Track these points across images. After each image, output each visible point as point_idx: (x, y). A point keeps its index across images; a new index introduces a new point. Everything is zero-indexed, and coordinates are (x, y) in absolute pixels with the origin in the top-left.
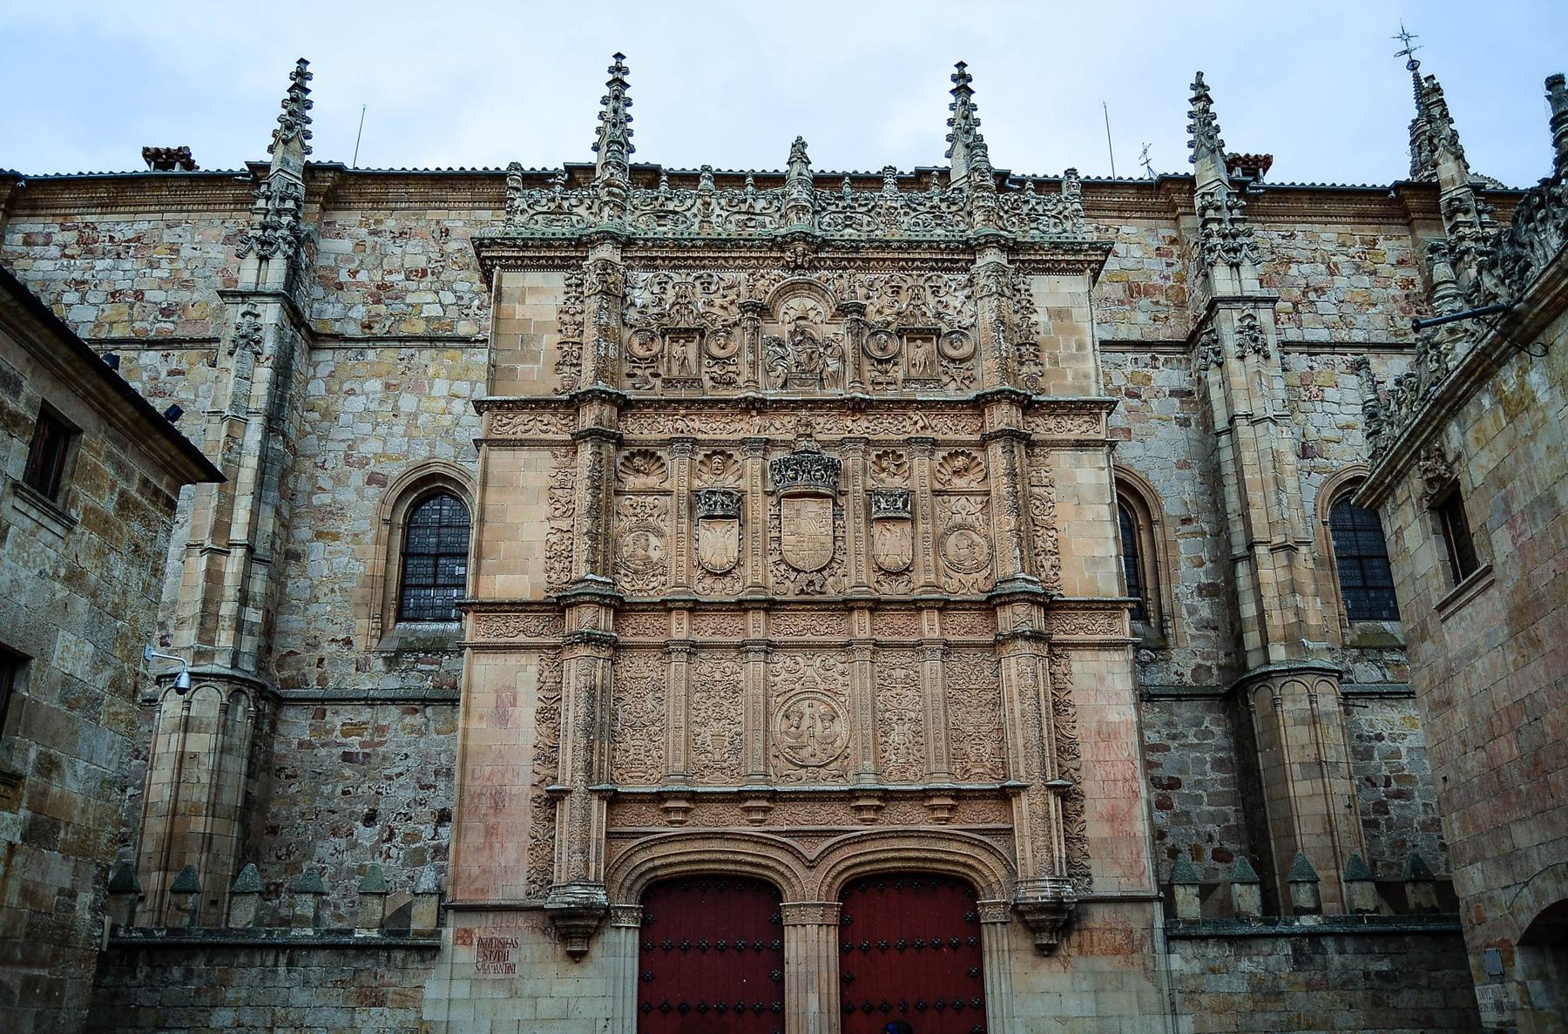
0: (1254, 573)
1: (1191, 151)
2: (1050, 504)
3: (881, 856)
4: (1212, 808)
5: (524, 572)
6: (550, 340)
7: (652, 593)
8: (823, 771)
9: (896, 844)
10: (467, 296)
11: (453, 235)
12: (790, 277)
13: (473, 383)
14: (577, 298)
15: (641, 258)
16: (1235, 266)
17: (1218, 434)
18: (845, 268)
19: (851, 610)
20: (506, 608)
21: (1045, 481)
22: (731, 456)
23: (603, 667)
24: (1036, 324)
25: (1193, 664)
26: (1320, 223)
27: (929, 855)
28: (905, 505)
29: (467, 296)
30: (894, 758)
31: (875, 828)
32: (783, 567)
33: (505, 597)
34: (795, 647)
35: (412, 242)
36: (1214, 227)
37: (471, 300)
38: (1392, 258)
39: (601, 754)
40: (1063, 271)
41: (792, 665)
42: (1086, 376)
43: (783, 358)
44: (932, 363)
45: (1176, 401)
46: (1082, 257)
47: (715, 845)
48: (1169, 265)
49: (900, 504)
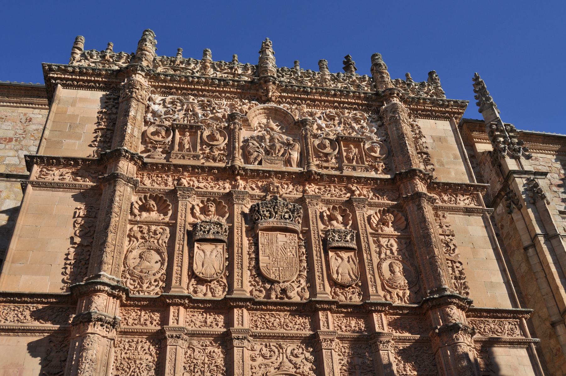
1: (478, 108)
7: (152, 293)
11: (34, 121)
12: (261, 106)
14: (114, 106)
15: (162, 87)
16: (517, 159)
17: (526, 249)
18: (299, 104)
21: (448, 233)
22: (220, 202)
26: (550, 154)
28: (352, 239)
35: (6, 123)
36: (502, 139)
41: (269, 353)
43: (258, 148)
44: (361, 158)
49: (348, 238)
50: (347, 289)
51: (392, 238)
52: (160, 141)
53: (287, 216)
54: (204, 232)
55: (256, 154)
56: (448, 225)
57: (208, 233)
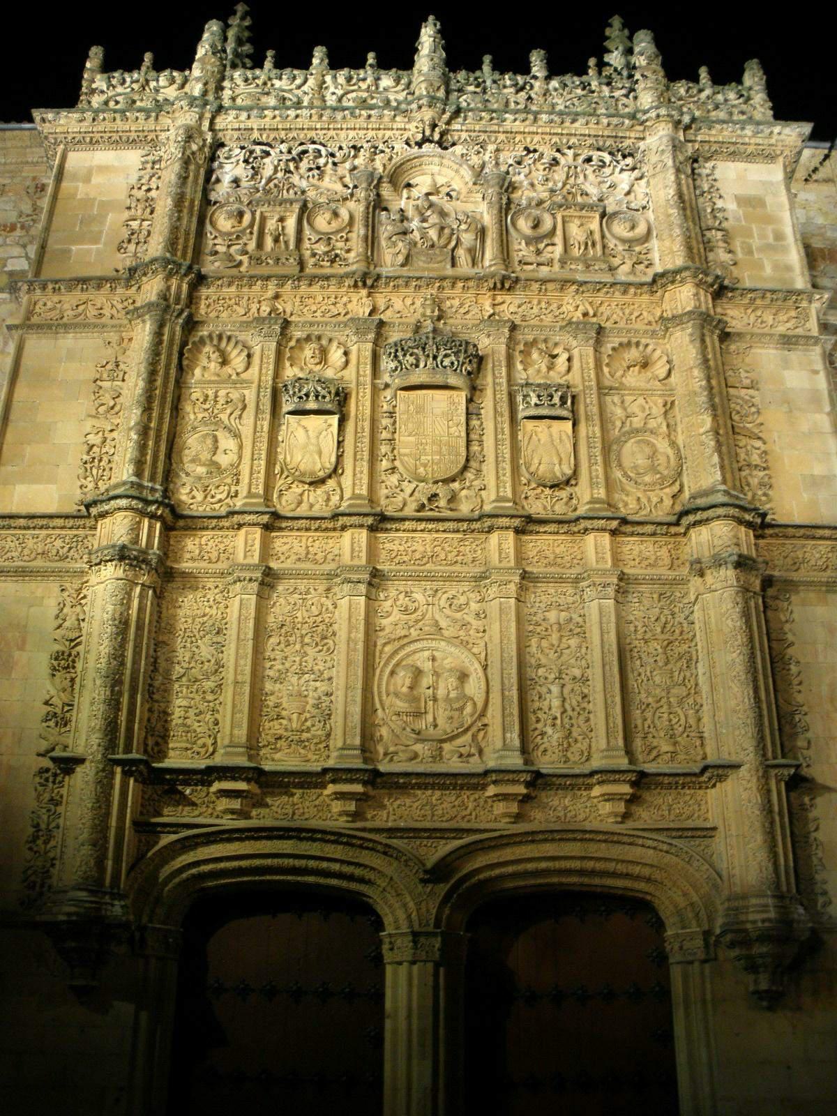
2: (753, 409)
3: (530, 866)
5: (51, 480)
6: (114, 219)
7: (217, 506)
8: (447, 746)
9: (549, 849)
19: (490, 530)
20: (22, 522)
21: (747, 382)
23: (141, 596)
27: (599, 866)
28: (563, 400)
30: (549, 730)
32: (394, 479)
33: (23, 511)
34: (410, 578)
39: (131, 712)
40: (750, 157)
42: (789, 268)
46: (773, 141)
47: (286, 846)
49: (556, 400)
50: (547, 491)
51: (641, 395)
52: (230, 234)
53: (447, 362)
54: (301, 398)
55: (400, 244)
56: (748, 369)
57: (307, 400)
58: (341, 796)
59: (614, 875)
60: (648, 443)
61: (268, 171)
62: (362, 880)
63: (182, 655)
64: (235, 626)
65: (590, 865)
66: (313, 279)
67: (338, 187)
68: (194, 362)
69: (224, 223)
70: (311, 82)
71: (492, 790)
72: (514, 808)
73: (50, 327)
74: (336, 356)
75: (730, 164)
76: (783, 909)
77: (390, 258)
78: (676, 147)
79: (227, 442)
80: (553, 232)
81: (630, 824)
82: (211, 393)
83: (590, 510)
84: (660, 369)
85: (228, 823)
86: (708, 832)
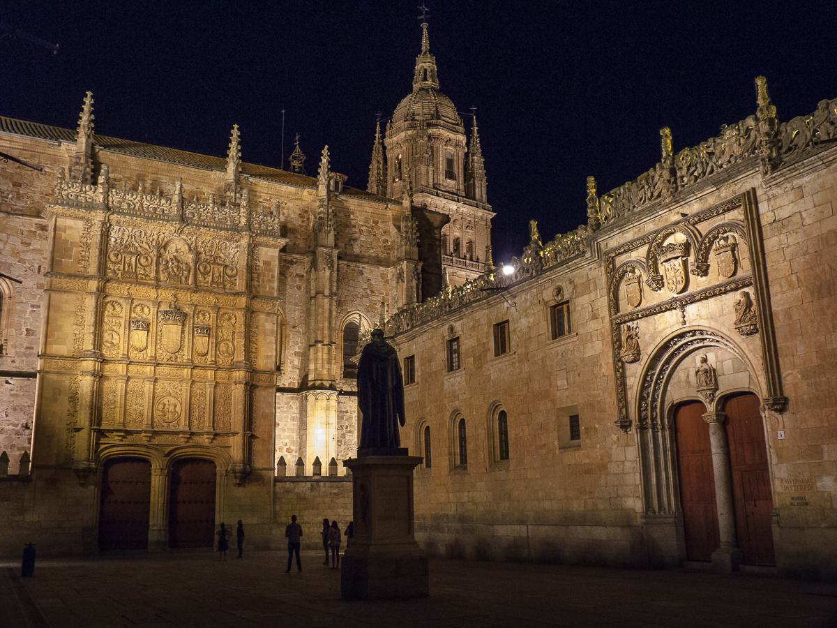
0: (316, 353)
4: (288, 434)
10: (6, 192)
13: (9, 235)
24: (259, 266)
25: (289, 382)
28: (207, 331)
29: (6, 192)
31: (187, 445)
32: (161, 351)
37: (8, 195)
38: (381, 231)
42: (273, 288)
45: (297, 279)
48: (303, 221)
52: (114, 263)
58: (146, 436)
59: (205, 455)
60: (228, 344)
61: (126, 238)
62: (149, 456)
63: (105, 399)
64: (119, 391)
65: (202, 453)
66: (140, 284)
67: (148, 248)
68: (105, 308)
69: (112, 257)
70: (138, 198)
71: (181, 435)
72: (186, 440)
73: (59, 291)
74: (146, 310)
75: (264, 248)
76: (244, 467)
77: (163, 277)
78: (249, 245)
79: (116, 336)
80: (209, 272)
81: (213, 444)
82: (111, 320)
83: (211, 364)
84: (233, 321)
85: (118, 443)
86: (230, 447)
